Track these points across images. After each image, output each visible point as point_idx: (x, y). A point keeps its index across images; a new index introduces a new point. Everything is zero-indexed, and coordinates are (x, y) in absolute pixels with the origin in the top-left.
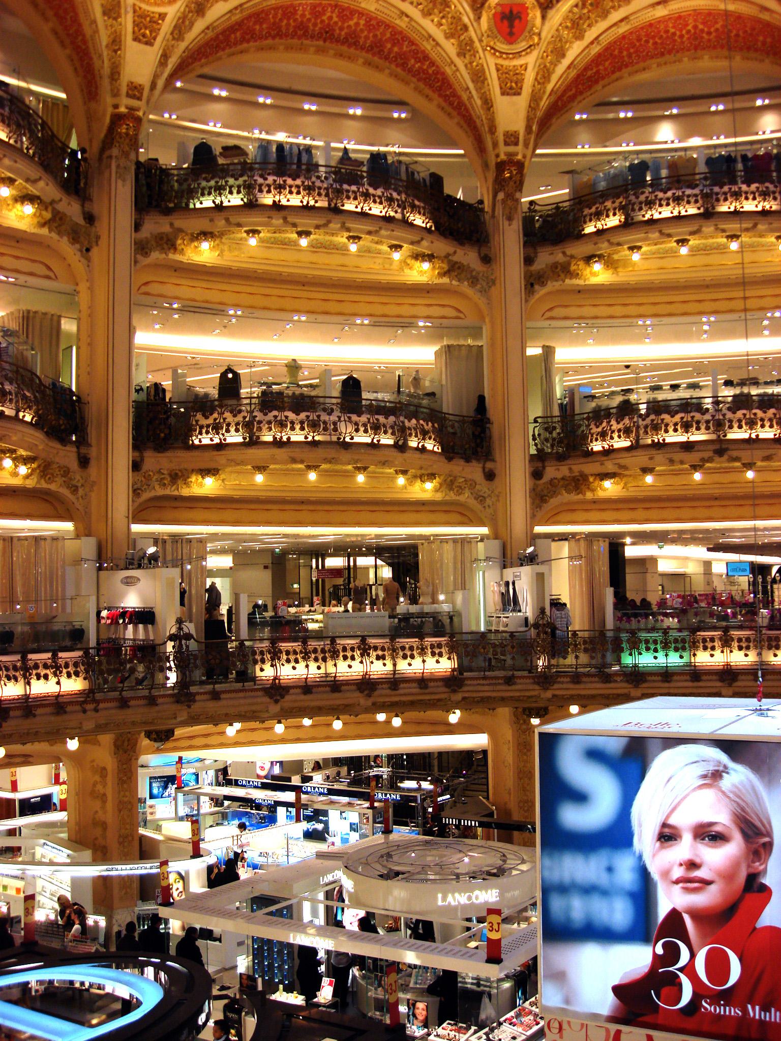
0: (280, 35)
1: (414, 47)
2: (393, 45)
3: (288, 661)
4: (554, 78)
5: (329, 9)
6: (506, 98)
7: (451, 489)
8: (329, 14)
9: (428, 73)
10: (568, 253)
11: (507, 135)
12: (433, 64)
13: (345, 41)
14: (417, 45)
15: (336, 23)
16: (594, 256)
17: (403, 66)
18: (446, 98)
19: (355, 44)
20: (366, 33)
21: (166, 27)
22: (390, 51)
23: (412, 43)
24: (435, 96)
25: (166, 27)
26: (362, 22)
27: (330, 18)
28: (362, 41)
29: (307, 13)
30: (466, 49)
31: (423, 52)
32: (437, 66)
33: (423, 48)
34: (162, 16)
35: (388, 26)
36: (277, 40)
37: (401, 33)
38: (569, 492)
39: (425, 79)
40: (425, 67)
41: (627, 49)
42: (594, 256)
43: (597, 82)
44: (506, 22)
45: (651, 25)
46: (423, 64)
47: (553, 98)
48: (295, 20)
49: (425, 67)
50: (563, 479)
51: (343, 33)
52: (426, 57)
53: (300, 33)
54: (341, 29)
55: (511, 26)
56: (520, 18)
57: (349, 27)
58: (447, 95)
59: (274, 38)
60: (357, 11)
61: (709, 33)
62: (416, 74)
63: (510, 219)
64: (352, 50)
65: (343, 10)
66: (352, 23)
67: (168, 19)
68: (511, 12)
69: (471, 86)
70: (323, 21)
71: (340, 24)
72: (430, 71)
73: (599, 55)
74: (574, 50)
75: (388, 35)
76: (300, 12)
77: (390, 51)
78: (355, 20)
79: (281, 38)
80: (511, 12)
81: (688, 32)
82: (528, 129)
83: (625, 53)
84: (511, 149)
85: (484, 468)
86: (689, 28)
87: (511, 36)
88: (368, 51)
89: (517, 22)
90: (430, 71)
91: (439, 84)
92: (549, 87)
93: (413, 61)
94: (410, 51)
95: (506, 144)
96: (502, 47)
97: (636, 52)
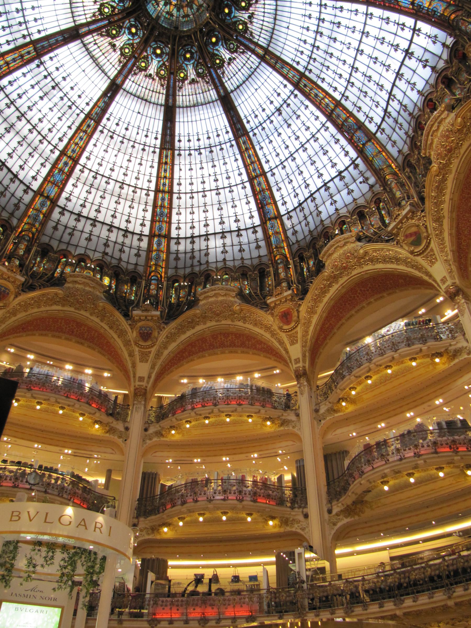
0: (204, 350)
3: (162, 606)
4: (310, 333)
6: (293, 347)
7: (287, 525)
11: (295, 360)
12: (265, 344)
13: (230, 346)
16: (340, 399)
17: (255, 348)
18: (274, 355)
19: (235, 346)
21: (152, 356)
23: (254, 338)
24: (271, 356)
25: (152, 356)
30: (273, 334)
34: (150, 352)
38: (346, 517)
42: (340, 399)
43: (332, 328)
45: (342, 297)
47: (313, 340)
50: (341, 511)
52: (262, 342)
55: (287, 319)
61: (368, 290)
63: (302, 394)
69: (279, 347)
73: (327, 317)
74: (315, 320)
82: (304, 356)
84: (298, 365)
85: (303, 512)
87: (288, 323)
92: (309, 337)
96: (285, 327)
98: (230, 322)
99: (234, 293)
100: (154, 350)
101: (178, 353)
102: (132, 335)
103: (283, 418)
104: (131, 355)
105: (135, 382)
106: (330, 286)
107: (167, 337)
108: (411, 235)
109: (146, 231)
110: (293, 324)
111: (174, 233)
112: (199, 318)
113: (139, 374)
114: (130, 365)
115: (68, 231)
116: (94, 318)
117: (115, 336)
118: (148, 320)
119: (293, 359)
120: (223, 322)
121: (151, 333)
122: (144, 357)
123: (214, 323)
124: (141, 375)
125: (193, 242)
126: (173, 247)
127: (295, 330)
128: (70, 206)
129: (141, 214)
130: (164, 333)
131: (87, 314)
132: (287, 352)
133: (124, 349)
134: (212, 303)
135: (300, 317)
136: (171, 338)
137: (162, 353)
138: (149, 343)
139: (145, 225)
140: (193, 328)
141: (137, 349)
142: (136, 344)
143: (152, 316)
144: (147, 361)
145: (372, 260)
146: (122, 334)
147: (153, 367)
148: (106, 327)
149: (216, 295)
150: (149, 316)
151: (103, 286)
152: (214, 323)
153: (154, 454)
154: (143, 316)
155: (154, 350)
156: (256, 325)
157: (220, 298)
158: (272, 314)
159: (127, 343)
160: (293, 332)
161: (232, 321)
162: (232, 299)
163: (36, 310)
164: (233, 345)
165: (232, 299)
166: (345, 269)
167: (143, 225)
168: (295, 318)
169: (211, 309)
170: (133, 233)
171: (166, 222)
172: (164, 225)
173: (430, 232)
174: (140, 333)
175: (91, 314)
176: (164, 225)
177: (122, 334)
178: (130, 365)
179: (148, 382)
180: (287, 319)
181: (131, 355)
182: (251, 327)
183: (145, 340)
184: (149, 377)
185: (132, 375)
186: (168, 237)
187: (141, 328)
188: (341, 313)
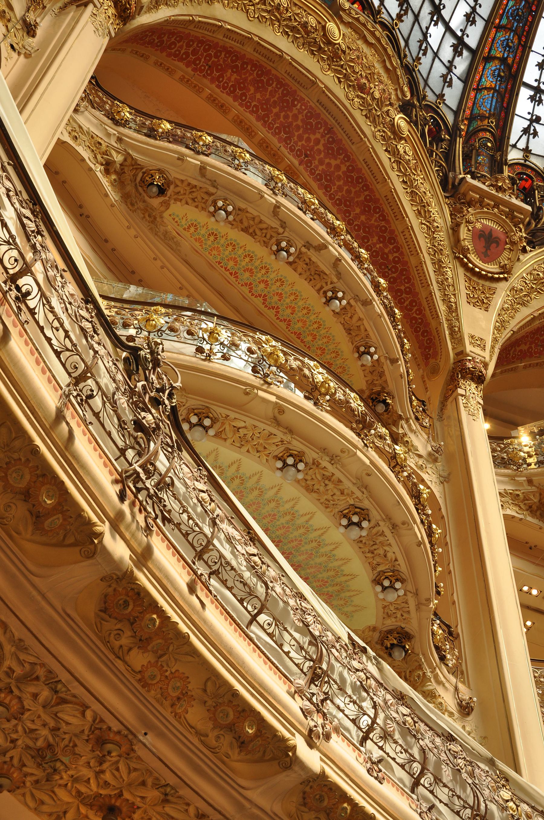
1: (383, 223)
2: (363, 212)
5: (322, 130)
8: (318, 136)
9: (387, 259)
10: (535, 483)
12: (397, 249)
14: (388, 222)
15: (319, 151)
20: (341, 183)
22: (357, 217)
23: (384, 218)
26: (344, 168)
27: (317, 142)
28: (334, 189)
29: (300, 117)
31: (392, 232)
32: (402, 254)
33: (393, 227)
35: (367, 187)
37: (377, 201)
39: (382, 264)
40: (386, 251)
44: (483, 243)
46: (386, 246)
48: (286, 117)
49: (386, 251)
51: (320, 168)
52: (392, 240)
53: (283, 135)
57: (329, 165)
58: (400, 291)
59: (258, 119)
60: (345, 151)
65: (334, 141)
66: (333, 162)
70: (308, 140)
71: (322, 155)
72: (391, 257)
75: (362, 198)
76: (295, 111)
77: (357, 217)
78: (338, 162)
89: (494, 245)
90: (391, 257)
91: (394, 275)
93: (375, 239)
94: (377, 227)
101: (229, 52)
110: (492, 268)
127: (494, 285)
160: (487, 284)
180: (487, 247)
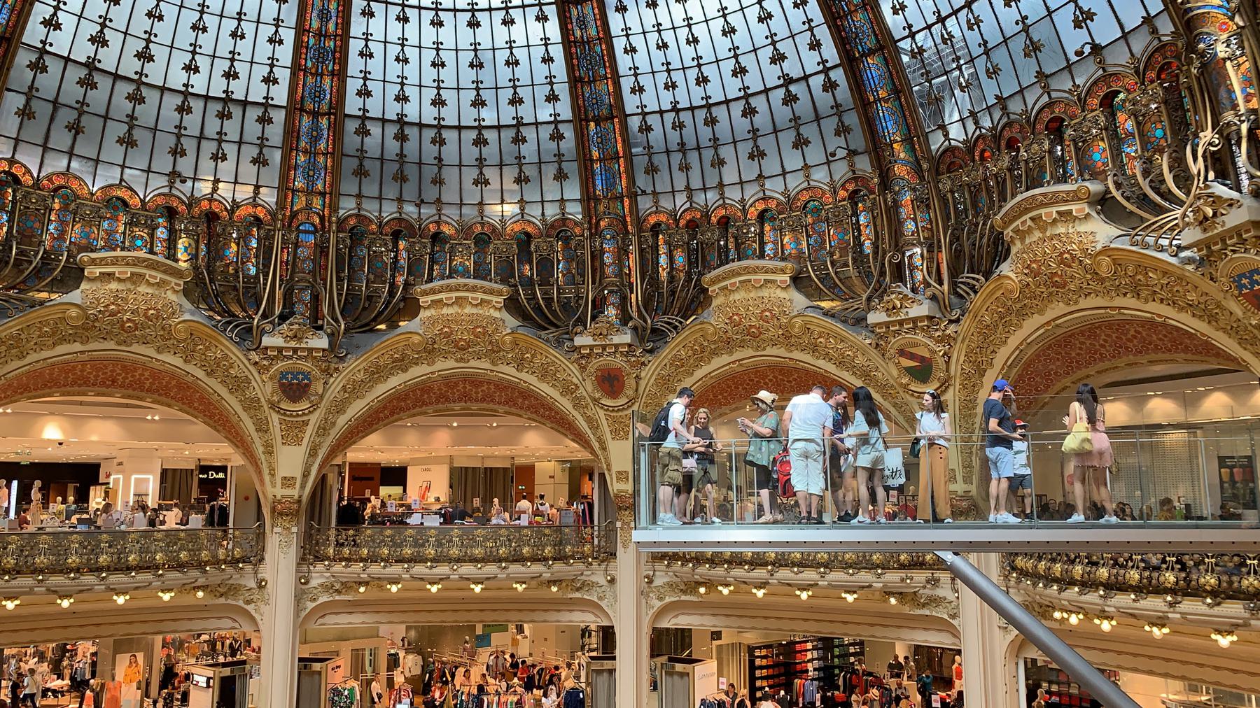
0: (424, 404)
22: (523, 403)
25: (310, 430)
26: (492, 387)
34: (306, 423)
36: (424, 408)
41: (721, 394)
54: (477, 393)
56: (618, 380)
62: (549, 418)
64: (491, 406)
66: (484, 388)
67: (311, 424)
68: (609, 374)
69: (589, 431)
79: (426, 405)
80: (609, 374)
81: (770, 380)
83: (720, 397)
86: (771, 377)
87: (614, 394)
88: (504, 405)
95: (619, 479)
97: (730, 395)
98: (487, 365)
99: (501, 299)
100: (314, 419)
102: (263, 388)
103: (583, 578)
104: (263, 428)
105: (274, 485)
106: (715, 353)
107: (344, 389)
108: (912, 356)
109: (280, 94)
110: (622, 401)
111: (353, 105)
112: (418, 352)
113: (282, 472)
114: (259, 449)
115: (66, 116)
116: (168, 358)
117: (223, 391)
118: (300, 358)
119: (614, 469)
120: (473, 363)
121: (308, 386)
122: (293, 432)
123: (451, 363)
124: (288, 475)
125: (401, 137)
126: (351, 141)
128: (60, 42)
129: (264, 50)
130: (336, 384)
131: (150, 351)
132: (604, 449)
133: (244, 416)
134: (449, 320)
135: (641, 390)
136: (354, 390)
137: (334, 424)
138: (304, 405)
139: (275, 81)
140: (405, 370)
141: (275, 418)
142: (274, 406)
143: (310, 350)
144: (298, 441)
145: (814, 349)
146: (239, 385)
147: (313, 453)
148: (200, 374)
149: (459, 302)
150: (303, 349)
151: (178, 273)
152: (451, 363)
153: (320, 621)
154: (287, 349)
155: (314, 419)
156: (543, 378)
157: (468, 310)
158: (583, 368)
159: (252, 405)
161: (493, 364)
162: (497, 314)
163: (16, 364)
164: (487, 398)
165: (497, 314)
166: (753, 336)
167: (270, 80)
168: (630, 392)
169: (447, 335)
170: (245, 104)
171: (332, 73)
172: (327, 83)
173: (952, 373)
174: (281, 385)
175: (159, 351)
176: (327, 83)
177: (239, 385)
178: (261, 449)
179: (303, 487)
180: (612, 386)
181: (263, 428)
182: (532, 379)
183: (294, 399)
184: (306, 475)
185: (266, 472)
186: (337, 109)
187: (283, 374)
188: (725, 398)
